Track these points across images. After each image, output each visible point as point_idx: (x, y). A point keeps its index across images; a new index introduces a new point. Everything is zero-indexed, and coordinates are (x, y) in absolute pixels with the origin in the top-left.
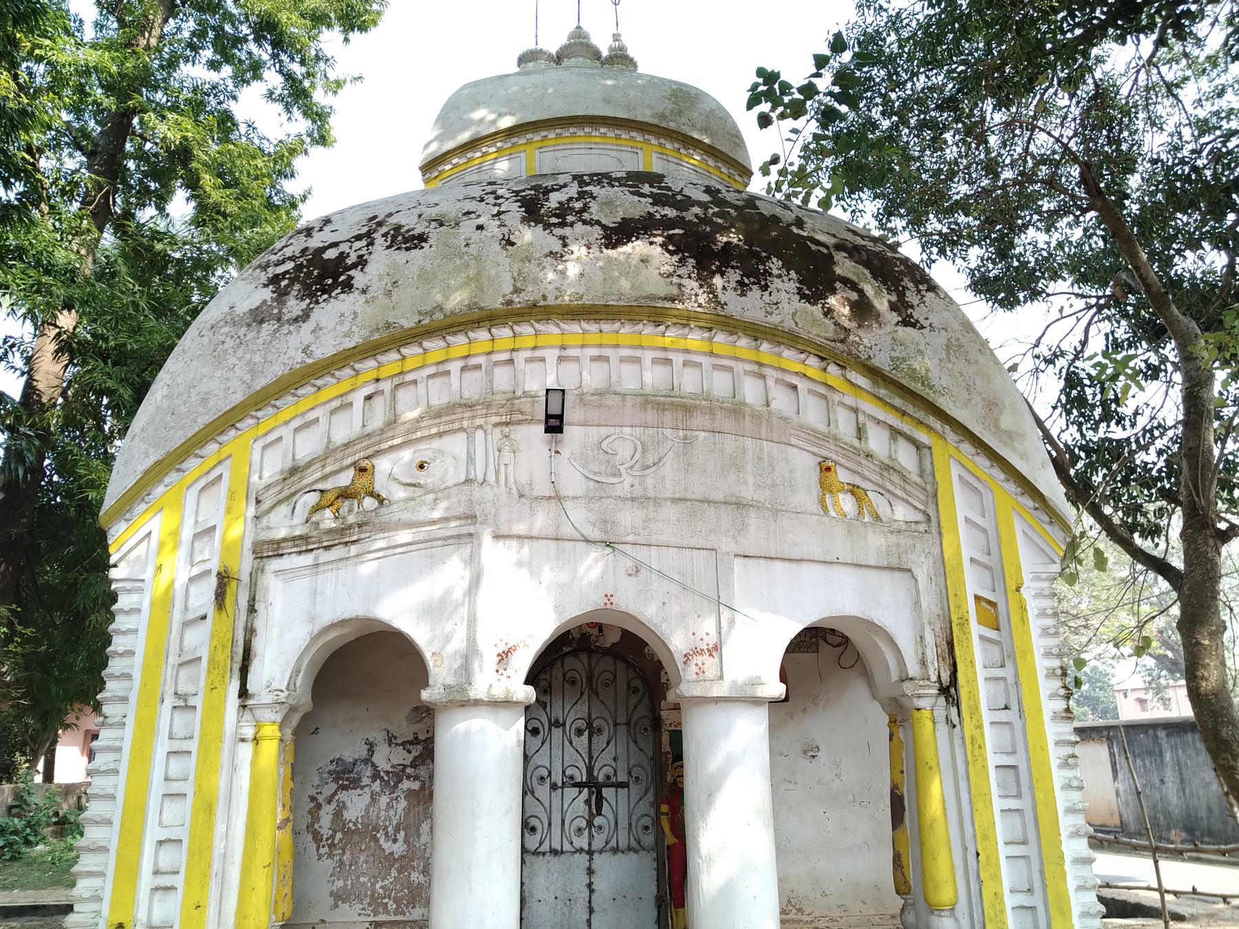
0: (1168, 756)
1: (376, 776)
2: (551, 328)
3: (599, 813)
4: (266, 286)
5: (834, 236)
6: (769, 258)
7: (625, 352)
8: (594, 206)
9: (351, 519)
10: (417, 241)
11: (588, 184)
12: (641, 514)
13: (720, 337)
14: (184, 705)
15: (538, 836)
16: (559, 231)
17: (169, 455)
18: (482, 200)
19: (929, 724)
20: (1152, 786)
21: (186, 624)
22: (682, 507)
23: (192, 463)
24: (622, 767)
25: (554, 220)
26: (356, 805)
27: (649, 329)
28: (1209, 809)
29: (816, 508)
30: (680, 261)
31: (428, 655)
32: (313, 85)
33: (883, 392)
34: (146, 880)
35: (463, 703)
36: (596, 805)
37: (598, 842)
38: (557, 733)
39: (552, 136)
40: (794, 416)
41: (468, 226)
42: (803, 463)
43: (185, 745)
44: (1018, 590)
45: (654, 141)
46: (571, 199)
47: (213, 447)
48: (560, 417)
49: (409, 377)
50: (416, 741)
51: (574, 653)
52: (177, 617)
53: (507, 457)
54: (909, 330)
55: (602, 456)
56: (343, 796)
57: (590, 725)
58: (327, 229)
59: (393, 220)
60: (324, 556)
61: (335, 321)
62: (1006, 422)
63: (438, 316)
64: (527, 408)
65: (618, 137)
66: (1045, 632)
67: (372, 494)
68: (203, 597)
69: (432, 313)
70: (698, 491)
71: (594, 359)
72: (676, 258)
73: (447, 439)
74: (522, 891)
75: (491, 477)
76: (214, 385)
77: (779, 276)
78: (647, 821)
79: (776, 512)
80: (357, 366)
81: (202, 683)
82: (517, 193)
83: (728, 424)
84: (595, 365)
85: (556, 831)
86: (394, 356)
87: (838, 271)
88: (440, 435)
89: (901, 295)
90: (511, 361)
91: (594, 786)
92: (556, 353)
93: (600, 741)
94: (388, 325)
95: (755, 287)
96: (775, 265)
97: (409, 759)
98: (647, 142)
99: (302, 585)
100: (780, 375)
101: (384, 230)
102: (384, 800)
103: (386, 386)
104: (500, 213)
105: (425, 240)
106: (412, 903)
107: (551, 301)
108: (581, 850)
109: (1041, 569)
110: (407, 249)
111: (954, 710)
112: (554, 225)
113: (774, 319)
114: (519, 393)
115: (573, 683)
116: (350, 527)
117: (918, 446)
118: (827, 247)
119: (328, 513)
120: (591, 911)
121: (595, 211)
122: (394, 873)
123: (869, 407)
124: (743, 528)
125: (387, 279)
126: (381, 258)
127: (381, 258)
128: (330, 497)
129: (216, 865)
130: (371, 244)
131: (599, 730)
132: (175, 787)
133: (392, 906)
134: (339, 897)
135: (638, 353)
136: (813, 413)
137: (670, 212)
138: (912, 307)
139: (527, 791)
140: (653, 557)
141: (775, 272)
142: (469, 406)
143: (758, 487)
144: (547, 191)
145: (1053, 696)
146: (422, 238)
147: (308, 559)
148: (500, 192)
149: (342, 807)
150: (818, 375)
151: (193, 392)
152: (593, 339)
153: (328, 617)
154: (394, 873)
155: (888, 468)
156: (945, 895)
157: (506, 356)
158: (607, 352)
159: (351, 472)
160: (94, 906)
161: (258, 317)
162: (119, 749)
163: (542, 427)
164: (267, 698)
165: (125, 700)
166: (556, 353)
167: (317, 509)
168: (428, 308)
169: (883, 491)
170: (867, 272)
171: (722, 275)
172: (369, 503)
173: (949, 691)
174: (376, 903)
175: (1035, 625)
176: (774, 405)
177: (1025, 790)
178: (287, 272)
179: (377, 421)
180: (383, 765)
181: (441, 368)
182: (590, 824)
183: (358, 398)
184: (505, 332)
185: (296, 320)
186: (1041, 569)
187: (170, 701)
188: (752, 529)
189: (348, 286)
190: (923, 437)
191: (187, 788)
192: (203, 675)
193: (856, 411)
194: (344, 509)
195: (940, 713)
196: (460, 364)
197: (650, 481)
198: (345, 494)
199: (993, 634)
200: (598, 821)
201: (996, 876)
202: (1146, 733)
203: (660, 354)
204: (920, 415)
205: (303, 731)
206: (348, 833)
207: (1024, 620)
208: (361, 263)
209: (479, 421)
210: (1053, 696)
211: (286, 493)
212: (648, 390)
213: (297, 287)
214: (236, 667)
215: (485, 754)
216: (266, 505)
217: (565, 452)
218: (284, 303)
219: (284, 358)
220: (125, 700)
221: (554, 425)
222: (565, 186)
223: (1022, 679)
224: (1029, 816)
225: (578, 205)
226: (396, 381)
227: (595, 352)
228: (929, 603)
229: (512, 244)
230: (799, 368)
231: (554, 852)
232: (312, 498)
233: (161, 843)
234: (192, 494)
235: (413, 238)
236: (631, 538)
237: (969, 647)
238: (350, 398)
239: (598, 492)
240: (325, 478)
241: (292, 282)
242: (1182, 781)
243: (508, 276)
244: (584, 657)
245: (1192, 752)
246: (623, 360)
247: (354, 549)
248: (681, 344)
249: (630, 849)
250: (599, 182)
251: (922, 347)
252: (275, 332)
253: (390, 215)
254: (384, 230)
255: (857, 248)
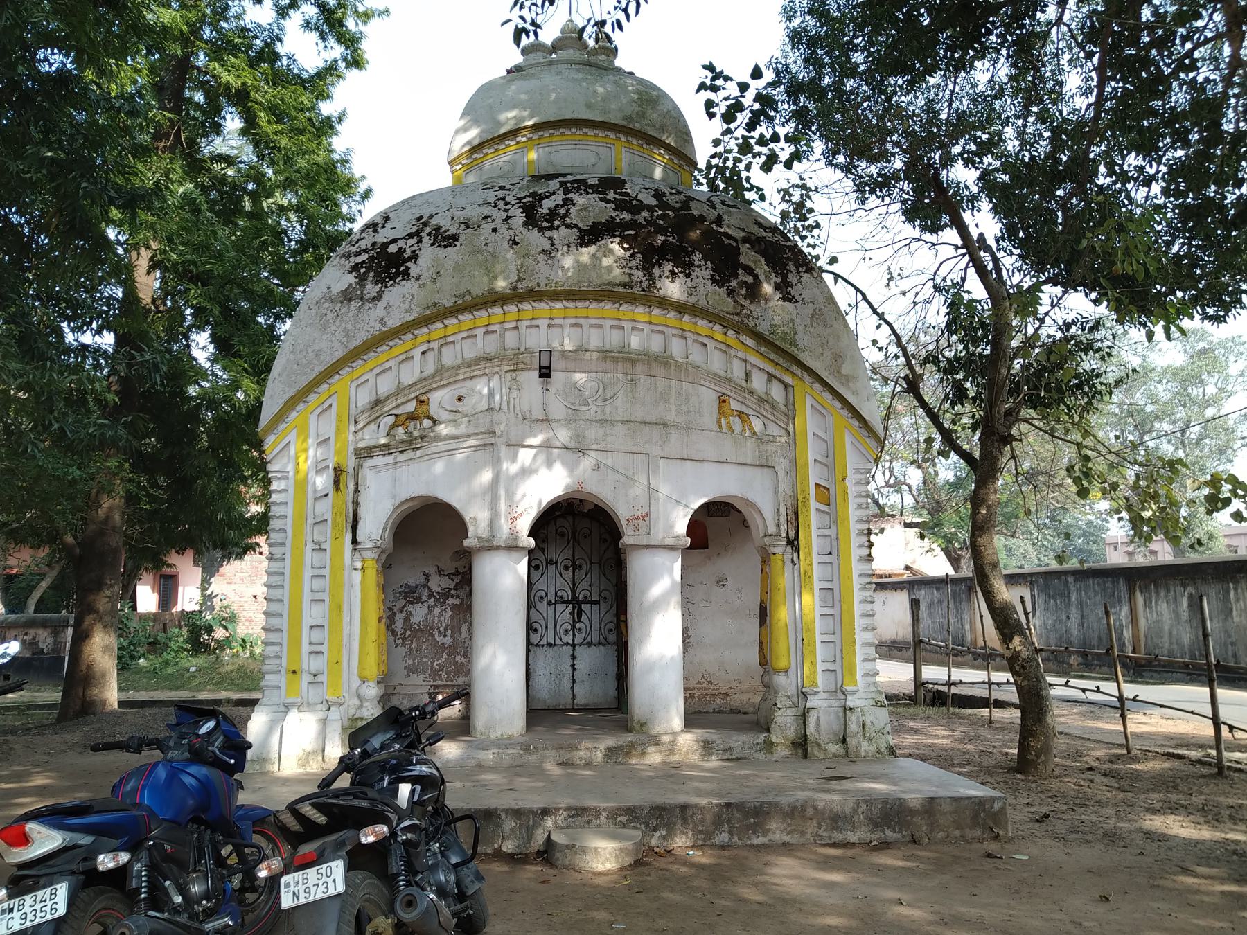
0: (1074, 598)
1: (431, 596)
2: (543, 305)
3: (580, 620)
4: (350, 272)
5: (743, 230)
6: (693, 252)
7: (593, 321)
8: (573, 210)
9: (416, 434)
10: (451, 240)
11: (570, 192)
12: (601, 431)
13: (656, 311)
14: (319, 548)
15: (539, 635)
16: (548, 234)
17: (299, 392)
18: (495, 206)
19: (780, 563)
20: (1061, 622)
21: (316, 499)
22: (628, 426)
23: (312, 397)
24: (595, 590)
25: (545, 224)
26: (419, 613)
27: (609, 305)
28: (1100, 638)
29: (715, 427)
30: (631, 256)
31: (467, 519)
32: (344, 14)
33: (763, 349)
34: (306, 648)
35: (489, 546)
36: (577, 615)
37: (579, 639)
38: (552, 568)
39: (546, 135)
40: (704, 366)
41: (486, 228)
42: (707, 396)
43: (322, 572)
44: (843, 480)
45: (623, 139)
46: (557, 206)
47: (325, 386)
48: (549, 368)
49: (449, 339)
50: (457, 573)
51: (563, 516)
52: (310, 494)
53: (515, 394)
54: (786, 304)
55: (577, 392)
56: (410, 608)
57: (574, 563)
58: (388, 225)
59: (433, 222)
60: (401, 458)
61: (400, 301)
62: (846, 369)
63: (468, 298)
64: (527, 361)
65: (596, 135)
66: (860, 507)
67: (429, 417)
68: (322, 482)
69: (463, 296)
70: (639, 416)
71: (572, 326)
72: (628, 254)
73: (474, 381)
74: (528, 664)
75: (505, 407)
76: (323, 345)
77: (699, 266)
78: (611, 626)
79: (688, 429)
80: (416, 332)
81: (329, 536)
82: (520, 199)
83: (659, 371)
84: (572, 329)
85: (551, 632)
86: (439, 325)
87: (742, 260)
88: (471, 378)
89: (785, 277)
90: (517, 328)
91: (576, 604)
92: (547, 322)
93: (580, 574)
94: (435, 305)
95: (681, 275)
96: (697, 257)
97: (453, 585)
98: (618, 139)
99: (388, 474)
100: (695, 337)
101: (428, 230)
102: (437, 611)
103: (435, 345)
104: (508, 218)
105: (457, 240)
106: (457, 675)
107: (543, 288)
108: (567, 644)
109: (861, 466)
110: (445, 247)
111: (795, 555)
112: (546, 228)
113: (693, 300)
114: (522, 350)
115: (563, 535)
116: (416, 439)
117: (786, 385)
118: (736, 241)
119: (401, 430)
120: (574, 681)
121: (574, 217)
122: (445, 656)
123: (754, 359)
124: (667, 440)
125: (432, 270)
126: (428, 254)
127: (428, 254)
128: (402, 419)
129: (345, 640)
130: (420, 241)
131: (580, 567)
132: (318, 596)
133: (444, 676)
134: (410, 670)
135: (601, 322)
136: (716, 362)
137: (626, 216)
138: (791, 286)
139: (530, 605)
140: (609, 460)
141: (697, 263)
142: (489, 359)
143: (678, 412)
144: (542, 198)
145: (861, 546)
146: (455, 238)
147: (390, 459)
148: (508, 199)
149: (409, 615)
150: (719, 337)
151: (310, 350)
152: (571, 313)
153: (404, 496)
154: (445, 656)
155: (761, 400)
156: (782, 663)
157: (513, 325)
158: (581, 321)
159: (414, 402)
160: (278, 662)
161: (347, 296)
162: (283, 574)
163: (537, 373)
164: (369, 545)
165: (283, 544)
166: (547, 322)
167: (394, 426)
168: (461, 292)
169: (759, 415)
170: (763, 260)
171: (660, 266)
172: (427, 423)
173: (793, 543)
174: (434, 674)
175: (852, 502)
176: (690, 357)
177: (837, 602)
178: (363, 262)
179: (430, 368)
180: (436, 589)
181: (471, 333)
182: (573, 627)
183: (417, 353)
184: (513, 308)
185: (373, 299)
186: (861, 466)
187: (310, 546)
188: (672, 441)
189: (406, 275)
190: (789, 379)
191: (325, 596)
192: (329, 531)
193: (746, 361)
194: (410, 428)
195: (788, 556)
196: (484, 330)
197: (608, 409)
198: (411, 417)
199: (825, 508)
200: (578, 625)
201: (813, 653)
202: (1059, 578)
203: (616, 323)
204: (787, 365)
205: (387, 565)
206: (413, 630)
207: (845, 499)
208: (414, 257)
209: (496, 369)
210: (861, 546)
211: (373, 416)
212: (608, 347)
213: (372, 274)
214: (349, 525)
215: (504, 580)
216: (361, 425)
217: (553, 389)
218: (364, 286)
219: (367, 327)
220: (283, 544)
221: (545, 372)
222: (554, 193)
223: (841, 537)
224: (837, 618)
225: (562, 211)
226: (441, 342)
227: (573, 321)
228: (785, 488)
229: (517, 244)
230: (708, 333)
231: (549, 645)
232: (390, 420)
233: (312, 627)
234: (314, 417)
235: (449, 237)
236: (595, 447)
237: (808, 516)
238: (411, 353)
239: (573, 419)
240: (398, 406)
241: (368, 269)
242: (1082, 617)
243: (514, 269)
244: (570, 518)
245: (1091, 593)
246: (591, 326)
247: (419, 453)
248: (629, 316)
249: (600, 643)
250: (579, 189)
251: (794, 316)
252: (361, 307)
253: (431, 216)
254: (428, 230)
255: (759, 240)
